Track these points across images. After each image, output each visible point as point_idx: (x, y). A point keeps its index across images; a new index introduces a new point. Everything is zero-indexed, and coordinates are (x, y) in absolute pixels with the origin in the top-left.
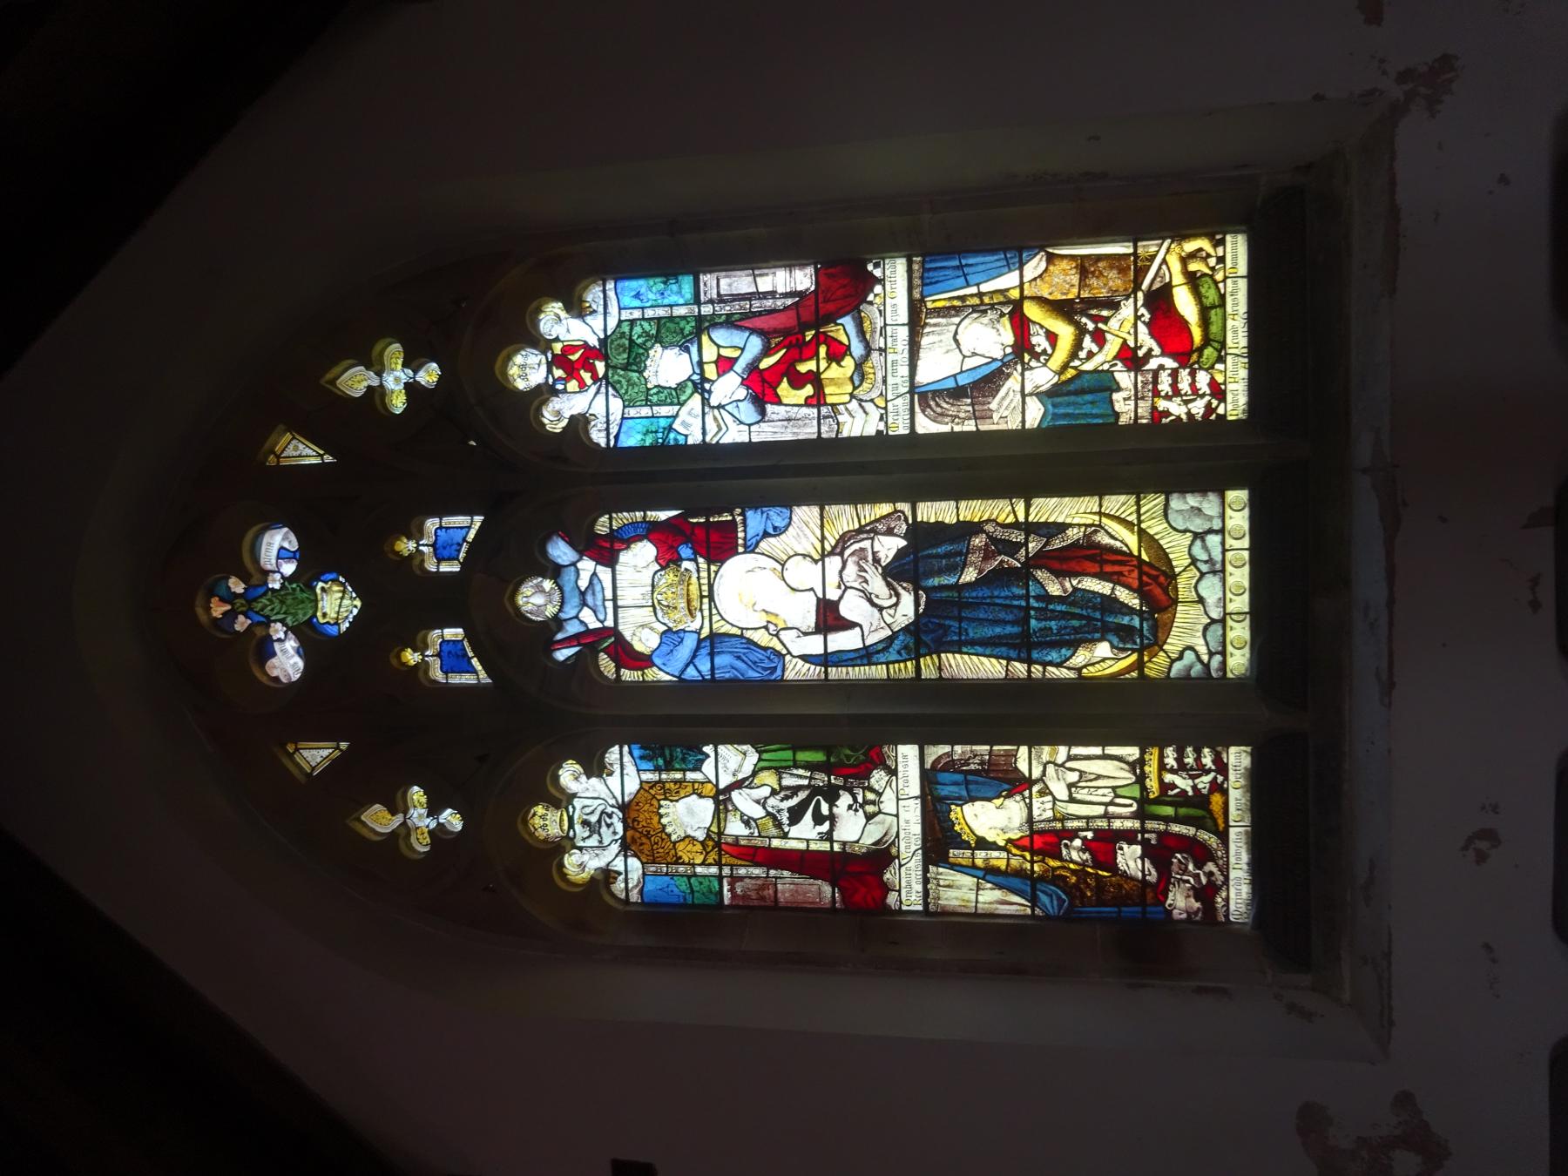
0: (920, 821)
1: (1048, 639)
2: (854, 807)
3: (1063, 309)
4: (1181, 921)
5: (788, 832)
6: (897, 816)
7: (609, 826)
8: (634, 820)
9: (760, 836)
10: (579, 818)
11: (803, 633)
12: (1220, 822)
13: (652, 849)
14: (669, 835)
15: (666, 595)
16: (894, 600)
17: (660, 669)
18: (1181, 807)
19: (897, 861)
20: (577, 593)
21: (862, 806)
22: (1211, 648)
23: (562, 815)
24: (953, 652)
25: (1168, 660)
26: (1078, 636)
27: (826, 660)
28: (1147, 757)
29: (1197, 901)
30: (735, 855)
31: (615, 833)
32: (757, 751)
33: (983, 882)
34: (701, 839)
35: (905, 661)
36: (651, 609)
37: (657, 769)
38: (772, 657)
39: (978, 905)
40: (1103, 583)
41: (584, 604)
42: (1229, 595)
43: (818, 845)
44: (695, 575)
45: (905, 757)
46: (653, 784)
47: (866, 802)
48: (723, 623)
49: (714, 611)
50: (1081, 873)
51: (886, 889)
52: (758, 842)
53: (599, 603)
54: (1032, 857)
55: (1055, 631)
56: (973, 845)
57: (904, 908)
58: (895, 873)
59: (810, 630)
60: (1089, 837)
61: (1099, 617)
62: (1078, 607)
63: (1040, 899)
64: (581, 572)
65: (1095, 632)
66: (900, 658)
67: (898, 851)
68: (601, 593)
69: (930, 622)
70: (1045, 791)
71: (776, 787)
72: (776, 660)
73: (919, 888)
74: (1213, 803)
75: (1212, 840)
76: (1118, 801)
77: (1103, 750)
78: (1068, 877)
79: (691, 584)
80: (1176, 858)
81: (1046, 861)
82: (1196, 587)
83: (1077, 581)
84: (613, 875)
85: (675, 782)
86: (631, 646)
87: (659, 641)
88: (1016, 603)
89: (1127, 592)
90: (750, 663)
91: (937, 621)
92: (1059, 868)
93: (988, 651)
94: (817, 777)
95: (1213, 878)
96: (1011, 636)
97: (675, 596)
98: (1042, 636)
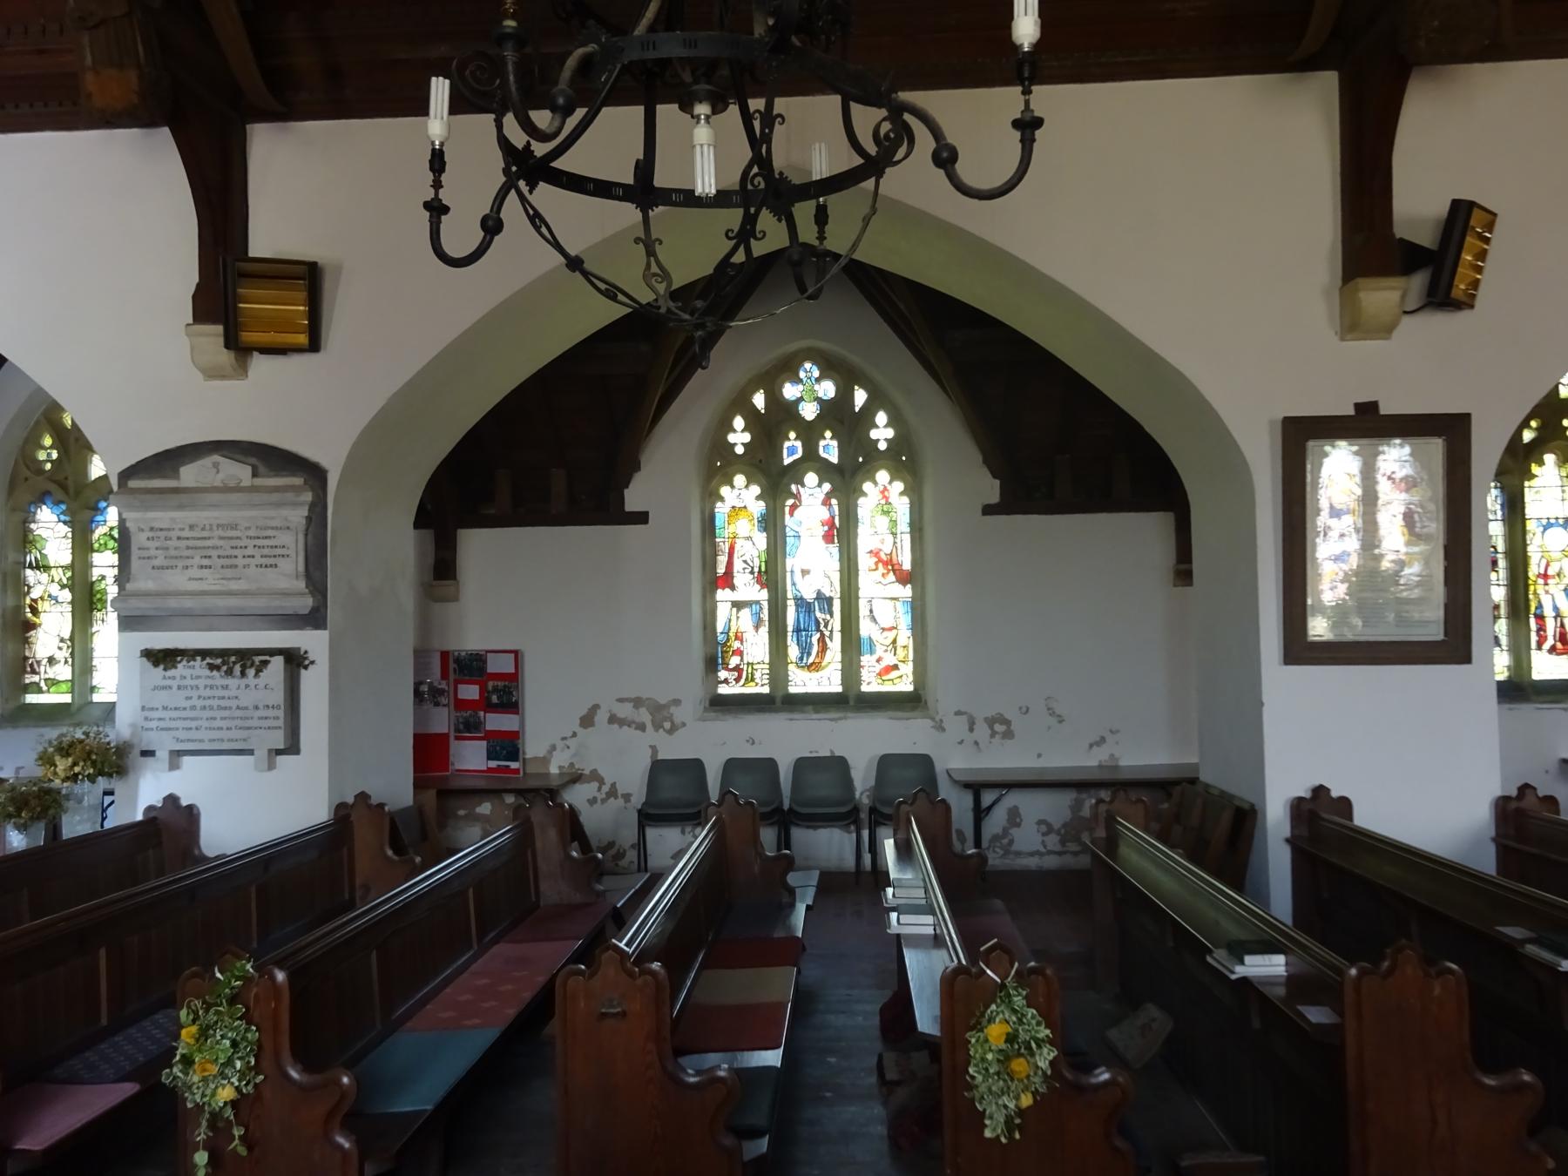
3: (894, 642)
27: (792, 572)
50: (730, 647)
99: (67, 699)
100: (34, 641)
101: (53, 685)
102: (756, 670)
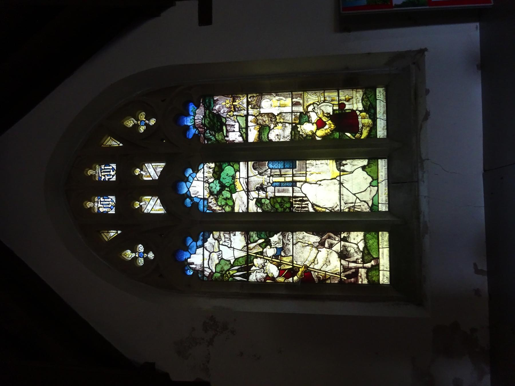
99: (384, 237)
100: (322, 274)
101: (369, 254)
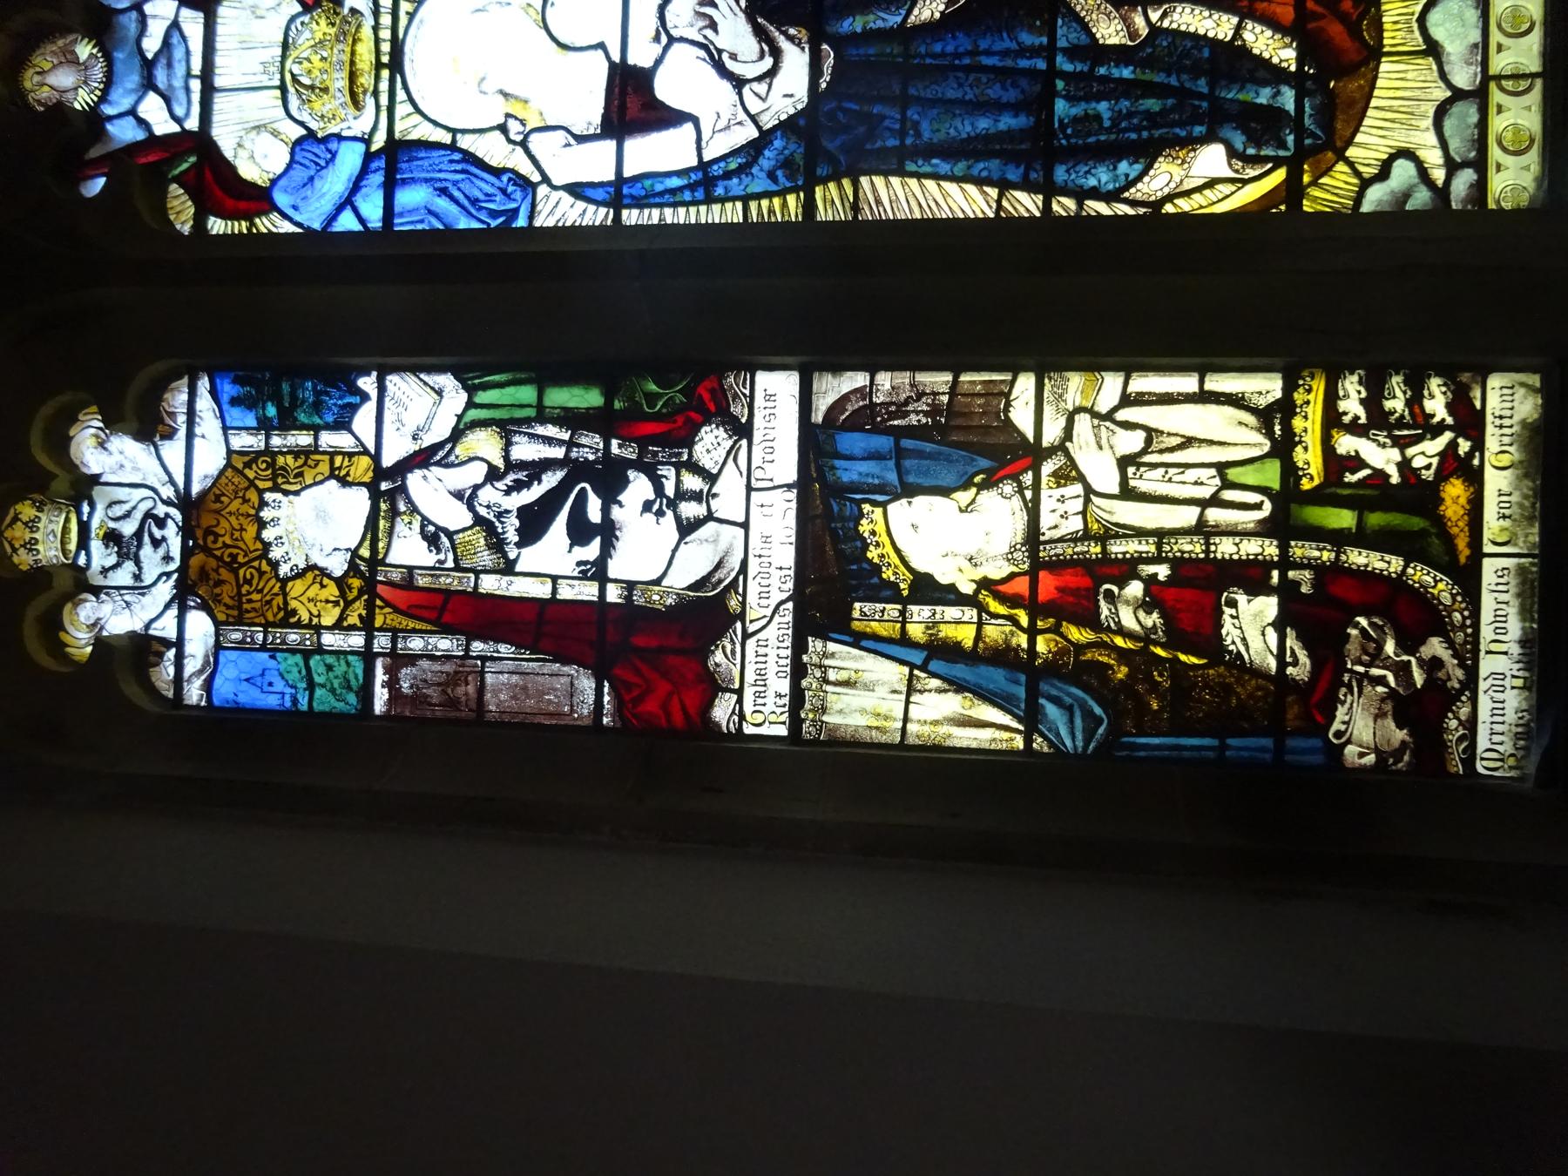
0: (793, 539)
1: (1091, 140)
2: (656, 507)
4: (1363, 769)
5: (515, 561)
6: (745, 525)
7: (156, 543)
8: (209, 531)
9: (457, 568)
10: (100, 527)
11: (575, 137)
12: (1462, 543)
13: (239, 594)
14: (275, 565)
15: (308, 63)
16: (768, 62)
17: (285, 216)
18: (1373, 510)
19: (739, 625)
20: (137, 61)
21: (673, 504)
22: (1452, 153)
23: (67, 520)
24: (886, 174)
25: (1355, 181)
26: (1157, 133)
27: (619, 192)
28: (1299, 397)
29: (1400, 726)
30: (403, 607)
31: (167, 558)
32: (465, 387)
33: (923, 675)
34: (338, 573)
35: (782, 193)
36: (278, 93)
37: (265, 426)
38: (510, 189)
39: (909, 726)
40: (1216, 16)
41: (149, 84)
42: (1496, 37)
43: (577, 589)
44: (369, 22)
45: (769, 397)
46: (252, 457)
47: (682, 495)
48: (417, 118)
49: (401, 95)
50: (1139, 660)
51: (713, 686)
52: (451, 581)
53: (178, 83)
54: (1032, 622)
55: (1107, 124)
56: (905, 593)
57: (748, 730)
58: (733, 652)
59: (591, 131)
60: (1161, 577)
61: (1205, 90)
62: (1160, 70)
63: (1045, 715)
64: (150, 22)
65: (1193, 124)
66: (774, 188)
67: (743, 603)
68: (184, 63)
69: (841, 109)
70: (1070, 474)
71: (500, 463)
72: (518, 195)
73: (784, 686)
74: (1448, 502)
75: (1441, 586)
76: (1228, 495)
77: (1202, 382)
78: (1110, 667)
79: (360, 40)
80: (1356, 625)
81: (1063, 630)
82: (1422, 20)
83: (1160, 13)
84: (156, 647)
85: (297, 452)
86: (231, 169)
87: (287, 158)
88: (1024, 63)
89: (1269, 33)
90: (466, 203)
91: (857, 108)
92: (1090, 645)
93: (960, 168)
94: (584, 441)
95: (1441, 675)
96: (1009, 135)
97: (326, 66)
98: (1076, 134)
102: (1336, 464)
